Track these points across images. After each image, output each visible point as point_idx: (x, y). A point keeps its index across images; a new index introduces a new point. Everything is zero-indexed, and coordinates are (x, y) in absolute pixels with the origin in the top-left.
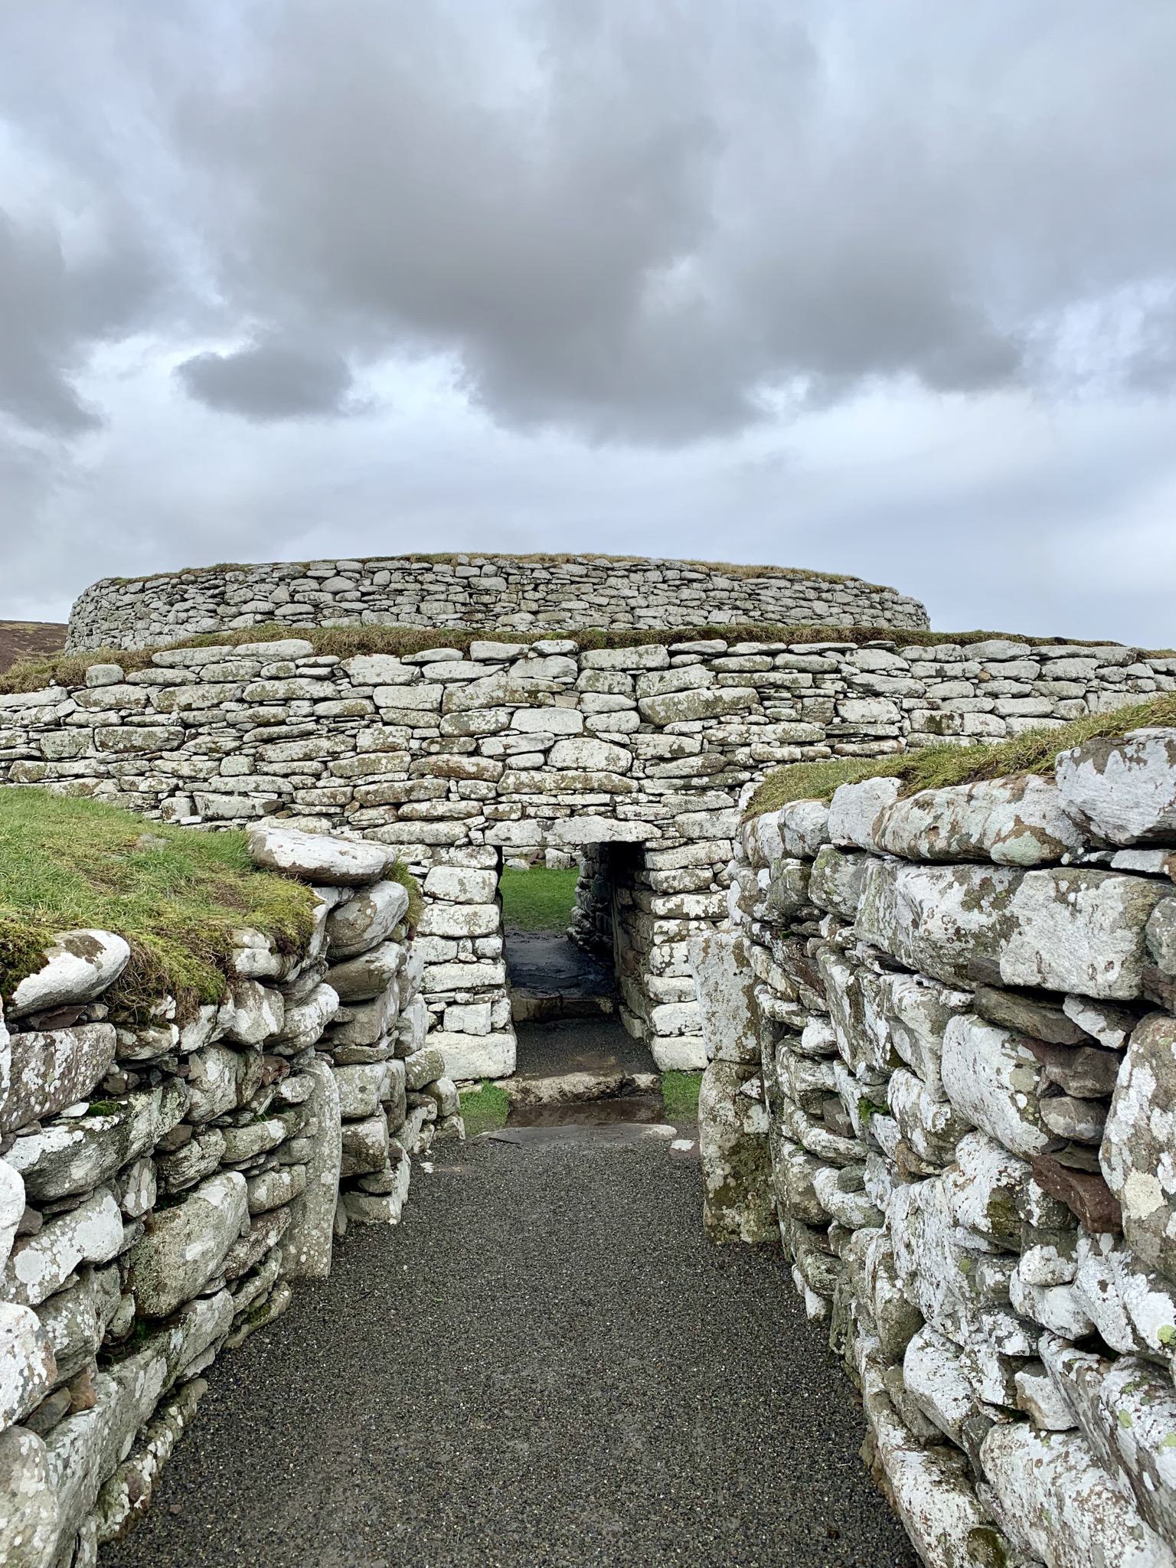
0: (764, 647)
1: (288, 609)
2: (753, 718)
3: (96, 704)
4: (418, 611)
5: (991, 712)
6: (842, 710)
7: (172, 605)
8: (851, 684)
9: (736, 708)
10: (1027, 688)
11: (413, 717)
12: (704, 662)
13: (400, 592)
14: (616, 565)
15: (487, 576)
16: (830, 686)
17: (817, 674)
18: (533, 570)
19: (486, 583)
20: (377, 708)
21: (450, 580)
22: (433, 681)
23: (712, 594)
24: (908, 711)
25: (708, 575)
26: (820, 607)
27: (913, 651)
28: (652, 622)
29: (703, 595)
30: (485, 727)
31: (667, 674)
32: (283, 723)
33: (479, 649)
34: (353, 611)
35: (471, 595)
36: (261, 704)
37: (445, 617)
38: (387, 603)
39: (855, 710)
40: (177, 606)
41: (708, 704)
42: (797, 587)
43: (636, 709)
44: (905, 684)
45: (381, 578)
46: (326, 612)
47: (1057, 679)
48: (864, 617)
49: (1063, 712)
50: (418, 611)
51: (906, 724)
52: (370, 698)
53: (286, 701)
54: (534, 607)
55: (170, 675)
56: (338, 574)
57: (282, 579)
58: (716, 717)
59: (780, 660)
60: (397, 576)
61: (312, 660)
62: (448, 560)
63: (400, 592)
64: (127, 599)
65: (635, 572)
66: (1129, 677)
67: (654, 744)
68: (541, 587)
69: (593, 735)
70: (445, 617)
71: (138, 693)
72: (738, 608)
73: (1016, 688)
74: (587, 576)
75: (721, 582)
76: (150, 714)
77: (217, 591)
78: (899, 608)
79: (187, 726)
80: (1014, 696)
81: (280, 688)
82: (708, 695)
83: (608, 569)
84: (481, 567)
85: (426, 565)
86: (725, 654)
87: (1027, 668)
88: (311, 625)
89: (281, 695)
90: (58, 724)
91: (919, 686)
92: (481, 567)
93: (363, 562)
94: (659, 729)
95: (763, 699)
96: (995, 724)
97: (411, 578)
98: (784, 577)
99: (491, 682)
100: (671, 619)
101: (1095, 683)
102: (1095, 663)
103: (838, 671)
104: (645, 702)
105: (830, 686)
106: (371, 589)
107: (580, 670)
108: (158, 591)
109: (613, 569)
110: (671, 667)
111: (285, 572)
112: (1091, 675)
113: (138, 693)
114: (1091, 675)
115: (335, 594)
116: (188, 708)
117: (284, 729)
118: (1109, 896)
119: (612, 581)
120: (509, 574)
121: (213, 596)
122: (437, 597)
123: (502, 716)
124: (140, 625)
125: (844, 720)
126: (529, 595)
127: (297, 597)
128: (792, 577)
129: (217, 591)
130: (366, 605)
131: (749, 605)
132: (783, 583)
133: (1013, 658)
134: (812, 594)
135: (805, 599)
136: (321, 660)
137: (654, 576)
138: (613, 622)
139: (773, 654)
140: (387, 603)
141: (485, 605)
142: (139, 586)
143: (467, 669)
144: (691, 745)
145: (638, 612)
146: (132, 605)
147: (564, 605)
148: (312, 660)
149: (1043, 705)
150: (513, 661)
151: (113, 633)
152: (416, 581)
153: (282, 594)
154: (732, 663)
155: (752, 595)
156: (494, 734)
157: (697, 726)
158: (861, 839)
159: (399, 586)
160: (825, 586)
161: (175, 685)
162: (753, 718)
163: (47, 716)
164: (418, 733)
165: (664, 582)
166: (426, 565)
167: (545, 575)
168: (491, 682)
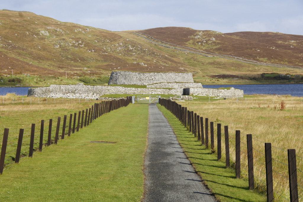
153: (149, 75)
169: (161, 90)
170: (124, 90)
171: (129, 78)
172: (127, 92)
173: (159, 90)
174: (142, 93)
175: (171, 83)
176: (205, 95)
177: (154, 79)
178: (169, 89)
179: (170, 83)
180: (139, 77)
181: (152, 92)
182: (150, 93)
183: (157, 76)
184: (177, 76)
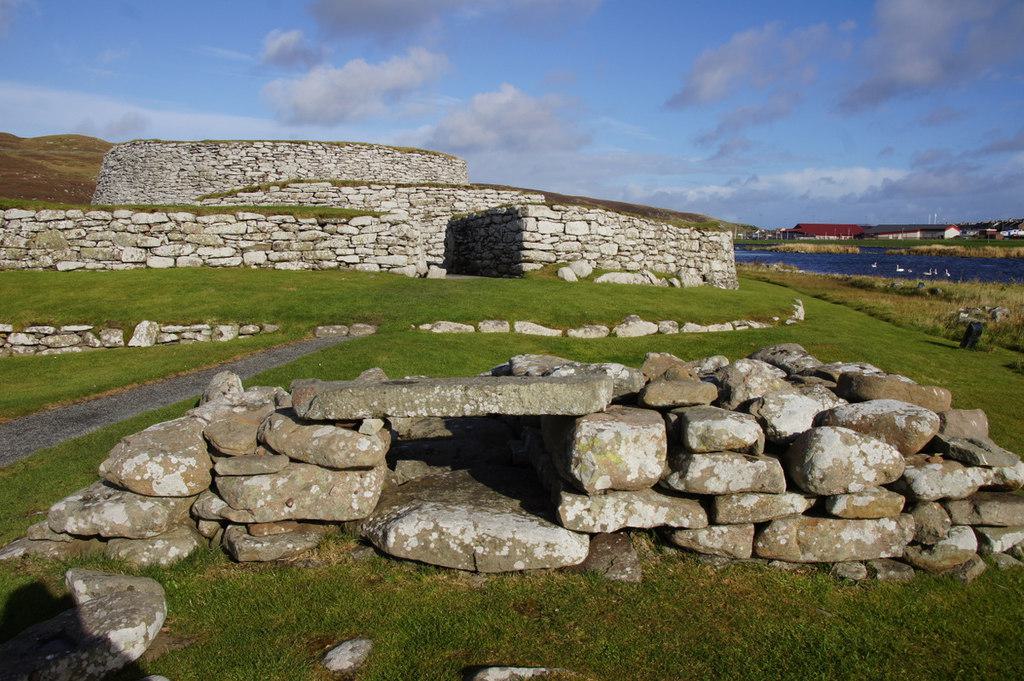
13: (288, 154)
16: (452, 199)
17: (449, 196)
33: (373, 186)
39: (457, 204)
44: (468, 199)
45: (280, 149)
54: (336, 161)
63: (288, 154)
67: (414, 211)
71: (286, 194)
75: (398, 154)
76: (289, 200)
81: (325, 194)
93: (274, 142)
108: (185, 148)
113: (286, 194)
131: (407, 163)
134: (428, 159)
137: (376, 151)
142: (175, 145)
144: (422, 211)
153: (243, 153)
155: (409, 160)
163: (260, 199)
168: (376, 195)
169: (241, 227)
171: (147, 172)
173: (225, 229)
174: (49, 261)
175: (361, 183)
176: (656, 281)
178: (326, 217)
179: (354, 184)
180: (191, 168)
181: (152, 242)
182: (130, 254)
183: (290, 159)
184: (397, 167)
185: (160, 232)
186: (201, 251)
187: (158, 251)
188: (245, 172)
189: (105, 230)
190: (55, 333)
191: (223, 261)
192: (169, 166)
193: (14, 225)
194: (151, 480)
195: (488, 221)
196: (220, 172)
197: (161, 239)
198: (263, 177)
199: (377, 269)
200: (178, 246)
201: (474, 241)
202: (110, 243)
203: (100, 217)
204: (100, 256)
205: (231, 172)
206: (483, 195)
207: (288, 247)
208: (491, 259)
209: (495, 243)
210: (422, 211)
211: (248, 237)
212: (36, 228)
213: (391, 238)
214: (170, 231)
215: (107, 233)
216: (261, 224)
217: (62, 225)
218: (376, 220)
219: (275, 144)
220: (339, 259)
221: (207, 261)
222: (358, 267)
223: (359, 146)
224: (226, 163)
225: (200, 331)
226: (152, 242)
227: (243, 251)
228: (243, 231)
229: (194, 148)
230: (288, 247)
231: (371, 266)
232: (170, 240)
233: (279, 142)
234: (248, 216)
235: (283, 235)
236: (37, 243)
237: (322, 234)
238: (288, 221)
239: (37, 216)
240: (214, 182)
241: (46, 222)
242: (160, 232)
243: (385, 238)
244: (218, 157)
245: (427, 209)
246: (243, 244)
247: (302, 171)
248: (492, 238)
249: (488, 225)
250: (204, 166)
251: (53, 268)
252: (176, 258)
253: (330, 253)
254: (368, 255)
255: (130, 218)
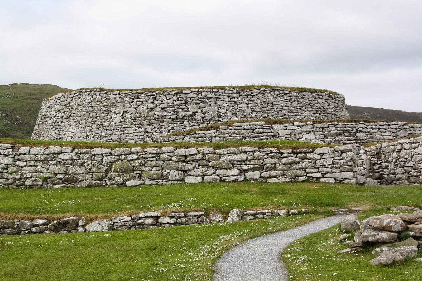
0: (344, 124)
1: (178, 102)
2: (343, 136)
3: (223, 133)
4: (216, 103)
5: (381, 135)
6: (357, 135)
7: (133, 99)
8: (358, 130)
9: (340, 134)
10: (386, 131)
11: (286, 136)
12: (334, 126)
13: (210, 98)
14: (267, 89)
15: (234, 93)
16: (355, 130)
17: (352, 128)
18: (246, 92)
19: (235, 95)
20: (279, 134)
21: (224, 94)
22: (289, 129)
23: (292, 97)
24: (367, 135)
25: (290, 92)
26: (319, 100)
27: (368, 124)
28: (278, 106)
29: (290, 98)
30: (299, 137)
31: (328, 128)
32: (262, 137)
33: (296, 124)
34: (197, 103)
35: (230, 99)
36: (257, 133)
37: (224, 105)
38: (207, 101)
39: (359, 134)
40: (135, 100)
41: (335, 134)
42: (313, 95)
43: (323, 134)
44: (367, 130)
45: (204, 94)
46: (189, 103)
47: (392, 129)
48: (331, 103)
49: (393, 135)
50: (216, 103)
51: (367, 137)
52: (278, 132)
53: (262, 133)
54: (247, 102)
55: (239, 128)
56: (191, 92)
57: (175, 94)
58: (336, 136)
59: (347, 126)
60: (209, 93)
61: (266, 125)
62: (223, 88)
64: (112, 96)
65: (272, 91)
66: (404, 128)
68: (249, 96)
69: (316, 139)
70: (224, 105)
71: (232, 131)
72: (298, 101)
73: (385, 130)
74: (260, 93)
75: (294, 94)
77: (155, 96)
78: (339, 99)
79: (243, 137)
80: (385, 132)
81: (261, 130)
82: (335, 132)
83: (265, 91)
84: (232, 91)
85: (217, 90)
86: (337, 125)
87: (386, 127)
88: (185, 107)
89: (261, 132)
90: (215, 137)
91: (368, 130)
92: (232, 91)
93: (198, 88)
94: (328, 138)
95: (344, 133)
96: (382, 137)
97: (213, 94)
98: (310, 92)
99: (299, 129)
100: (282, 105)
101: (398, 129)
102: (398, 126)
103: (355, 128)
104: (325, 133)
105: (355, 130)
106: (202, 97)
107: (314, 127)
109: (266, 91)
110: (328, 127)
111: (177, 92)
112: (398, 128)
114: (398, 128)
115: (190, 98)
116: (243, 134)
117: (263, 138)
118: (400, 145)
119: (266, 94)
120: (240, 93)
121: (153, 98)
122: (221, 99)
123: (301, 135)
124: (119, 105)
125: (357, 137)
126: (246, 99)
127: (180, 99)
128: (312, 91)
129: (155, 96)
130: (200, 102)
132: (310, 94)
133: (384, 125)
134: (317, 97)
135: (316, 98)
136: (268, 125)
137: (277, 92)
138: (268, 106)
139: (345, 125)
140: (207, 101)
141: (234, 102)
142: (118, 92)
143: (294, 127)
144: (333, 140)
145: (274, 103)
146: (115, 98)
147: (255, 102)
148: (266, 125)
149: (389, 134)
150: (302, 126)
151: (107, 107)
152: (215, 95)
153: (175, 98)
154: (339, 126)
155: (302, 98)
156: (301, 139)
157: (334, 137)
158: (385, 146)
159: (210, 96)
160: (320, 94)
161: (240, 130)
162: (343, 136)
163: (214, 135)
164: (287, 138)
165: (280, 94)
166: (217, 90)
167: (249, 93)
168: (299, 129)
169: (244, 156)
170: (8, 160)
171: (93, 115)
172: (28, 172)
173: (233, 157)
174: (120, 180)
177: (198, 117)
180: (133, 110)
181: (188, 167)
182: (174, 174)
183: (212, 102)
184: (294, 104)
185: (193, 161)
186: (218, 172)
187: (191, 173)
188: (177, 112)
189: (157, 160)
190: (185, 217)
191: (233, 178)
192: (114, 109)
193: (98, 158)
194: (391, 226)
195: (399, 147)
196: (157, 113)
197: (194, 165)
198: (192, 116)
199: (334, 181)
200: (204, 169)
201: (388, 161)
202: (160, 168)
203: (154, 152)
204: (155, 176)
205: (166, 113)
206: (377, 127)
207: (274, 168)
208: (403, 173)
209: (405, 162)
210: (333, 140)
211: (248, 163)
212: (113, 160)
213: (342, 161)
214: (199, 160)
215: (159, 162)
216: (256, 154)
217: (130, 157)
218: (332, 149)
219: (199, 91)
220: (308, 175)
221: (223, 178)
222: (322, 180)
223: (263, 89)
224: (162, 106)
225: (265, 214)
226: (188, 167)
227: (245, 171)
228: (244, 158)
229: (135, 94)
230: (274, 168)
231: (329, 179)
232: (199, 166)
233: (202, 88)
234: (248, 149)
235: (272, 161)
236: (113, 169)
237: (297, 160)
238: (274, 151)
239: (113, 152)
240: (153, 122)
241: (119, 155)
242: (193, 161)
243: (339, 161)
244: (155, 102)
245: (337, 139)
246: (245, 167)
247: (222, 110)
248: (404, 159)
249: (399, 151)
250: (144, 109)
251: (123, 184)
252: (203, 176)
253: (303, 172)
254: (327, 173)
255: (173, 152)
